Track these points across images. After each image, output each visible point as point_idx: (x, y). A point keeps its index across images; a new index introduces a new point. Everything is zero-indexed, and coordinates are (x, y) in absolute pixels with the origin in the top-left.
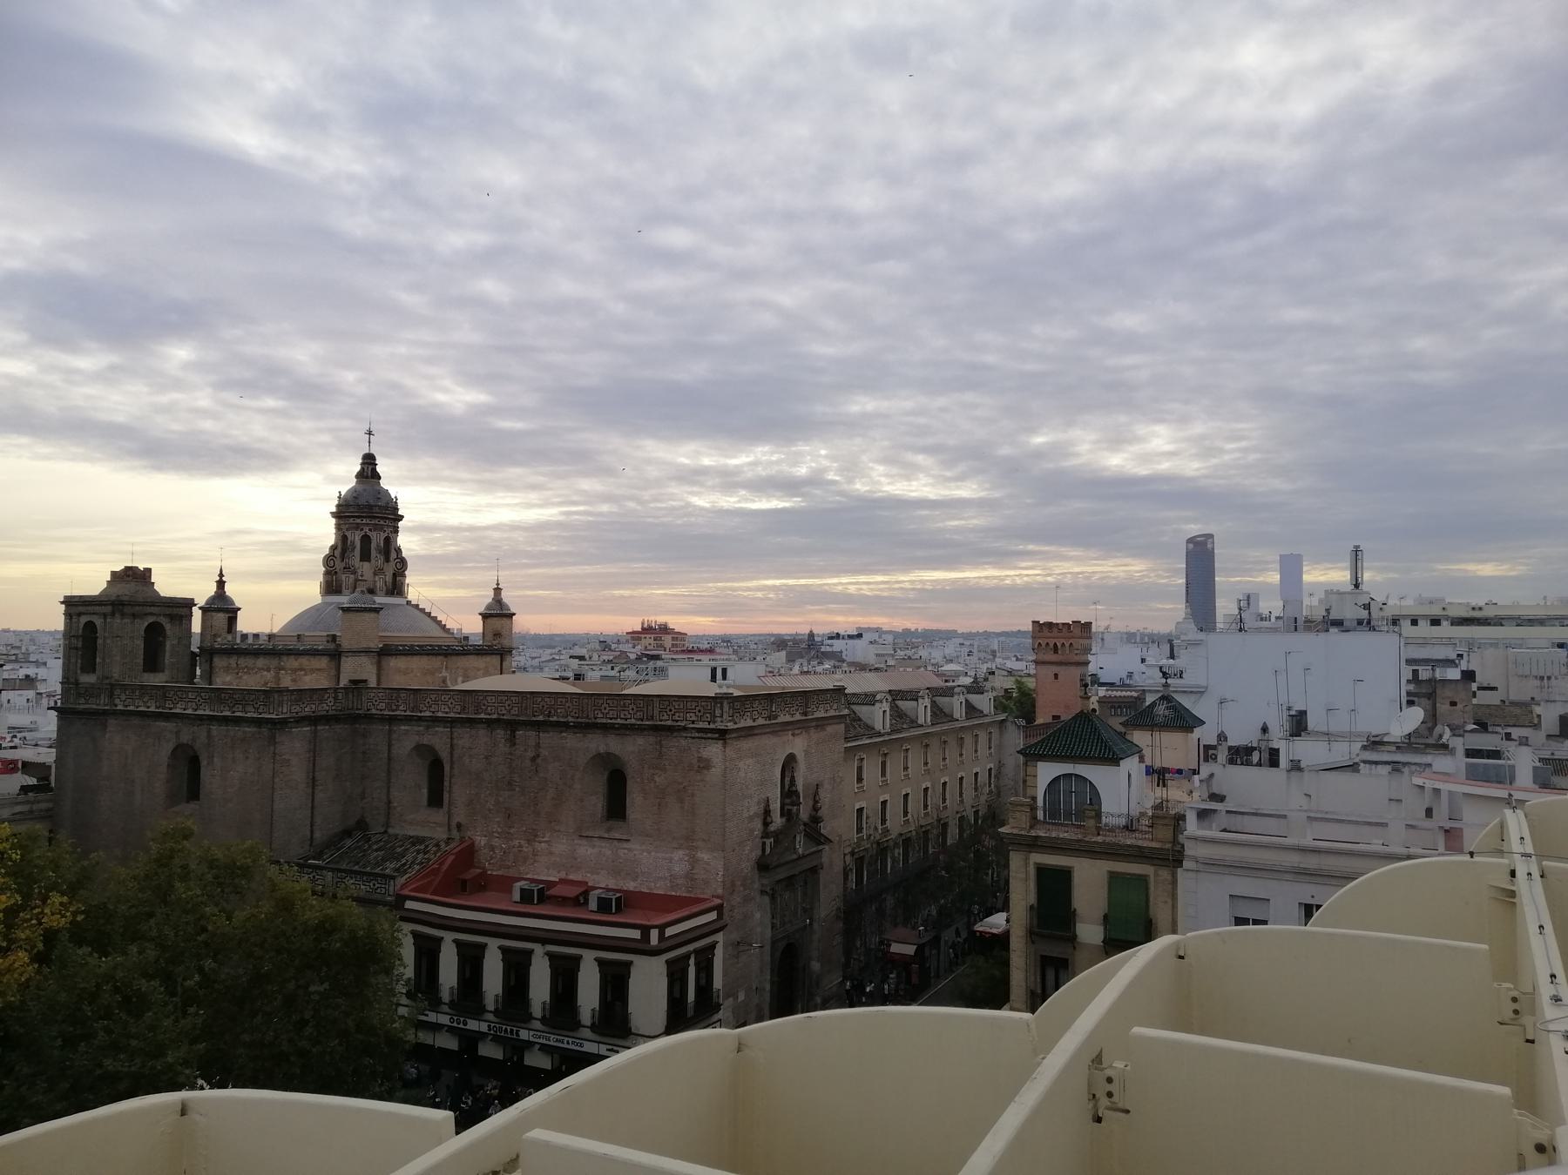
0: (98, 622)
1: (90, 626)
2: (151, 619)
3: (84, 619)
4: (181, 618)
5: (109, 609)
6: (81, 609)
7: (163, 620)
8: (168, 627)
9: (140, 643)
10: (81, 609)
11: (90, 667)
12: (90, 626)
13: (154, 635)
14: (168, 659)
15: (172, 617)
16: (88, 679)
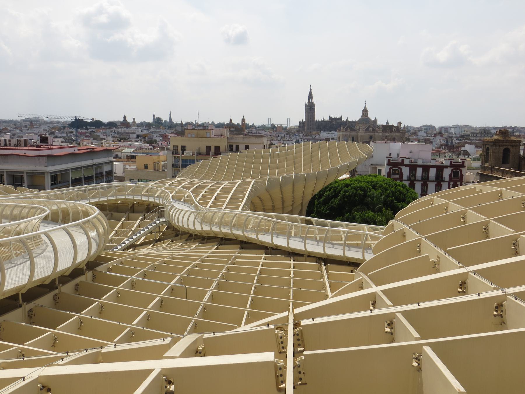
0: (490, 147)
1: (488, 148)
2: (505, 147)
3: (487, 146)
4: (516, 146)
5: (492, 144)
6: (486, 143)
7: (509, 147)
8: (511, 149)
9: (501, 155)
10: (486, 143)
11: (487, 161)
12: (488, 148)
13: (506, 152)
14: (511, 159)
15: (512, 146)
16: (487, 165)
